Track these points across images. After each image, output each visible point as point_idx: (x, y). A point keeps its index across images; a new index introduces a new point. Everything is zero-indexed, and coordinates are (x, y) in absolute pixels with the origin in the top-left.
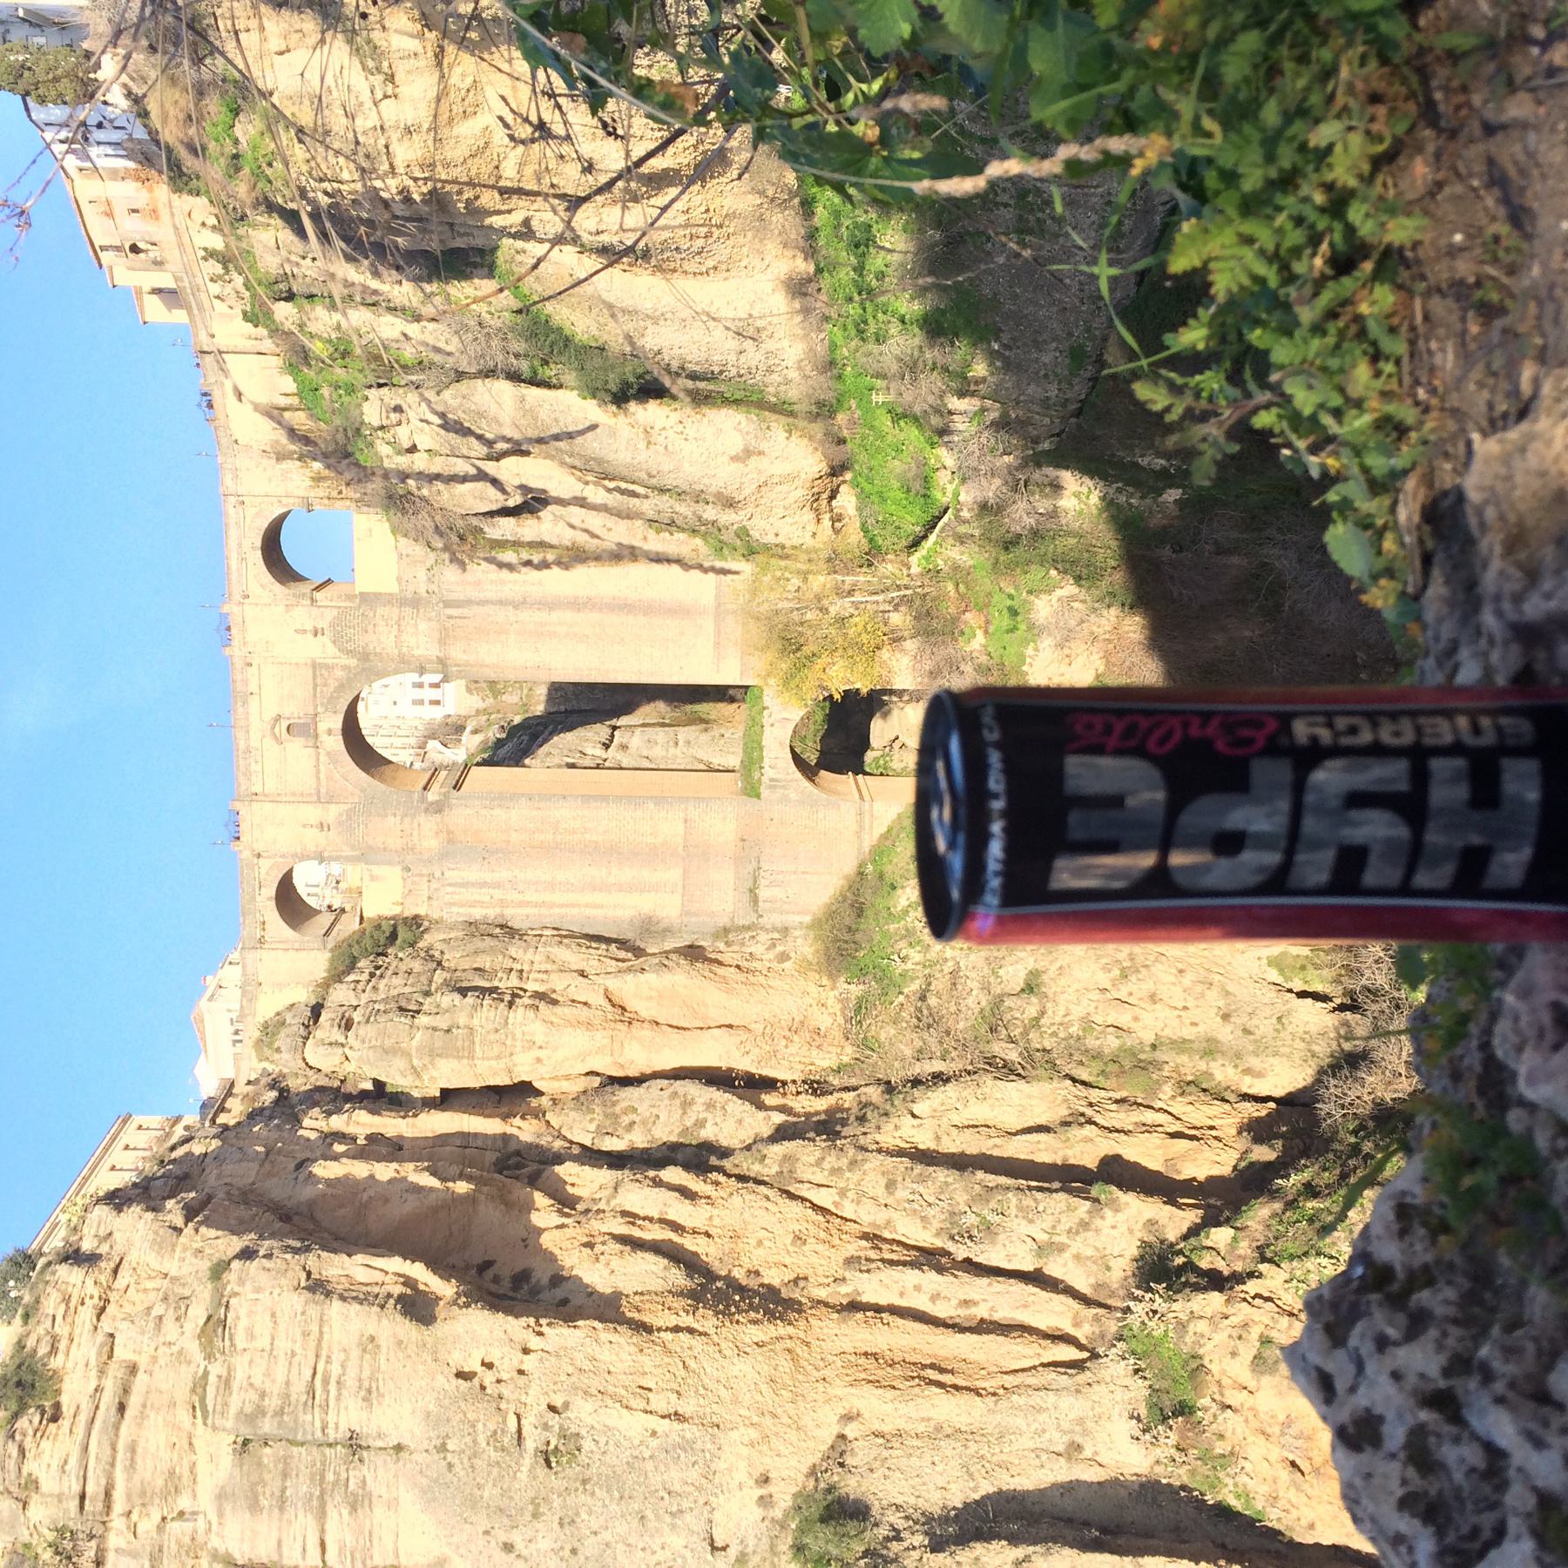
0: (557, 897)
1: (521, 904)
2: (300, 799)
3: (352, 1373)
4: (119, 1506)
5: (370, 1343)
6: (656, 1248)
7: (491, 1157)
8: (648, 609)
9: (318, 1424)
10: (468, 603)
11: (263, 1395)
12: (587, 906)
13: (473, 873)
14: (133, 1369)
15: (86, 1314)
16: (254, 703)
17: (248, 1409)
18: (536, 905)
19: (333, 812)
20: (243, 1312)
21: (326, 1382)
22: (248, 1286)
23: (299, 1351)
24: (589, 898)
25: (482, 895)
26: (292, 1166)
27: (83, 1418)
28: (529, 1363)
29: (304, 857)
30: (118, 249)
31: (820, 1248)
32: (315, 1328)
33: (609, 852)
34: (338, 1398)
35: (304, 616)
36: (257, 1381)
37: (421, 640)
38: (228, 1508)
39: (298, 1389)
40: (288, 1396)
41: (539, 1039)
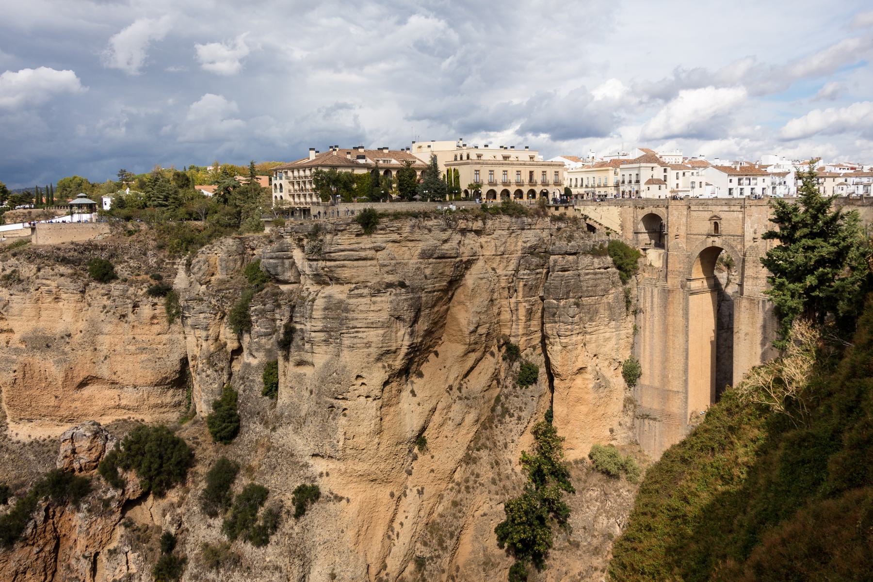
0: (647, 333)
1: (645, 318)
3: (358, 341)
5: (368, 345)
9: (343, 331)
11: (353, 311)
12: (644, 346)
13: (656, 300)
14: (372, 259)
17: (349, 307)
20: (383, 299)
21: (357, 332)
22: (393, 297)
24: (647, 347)
25: (648, 305)
26: (494, 266)
27: (355, 246)
28: (362, 399)
31: (431, 478)
32: (374, 326)
36: (360, 308)
38: (326, 300)
40: (353, 320)
41: (555, 348)
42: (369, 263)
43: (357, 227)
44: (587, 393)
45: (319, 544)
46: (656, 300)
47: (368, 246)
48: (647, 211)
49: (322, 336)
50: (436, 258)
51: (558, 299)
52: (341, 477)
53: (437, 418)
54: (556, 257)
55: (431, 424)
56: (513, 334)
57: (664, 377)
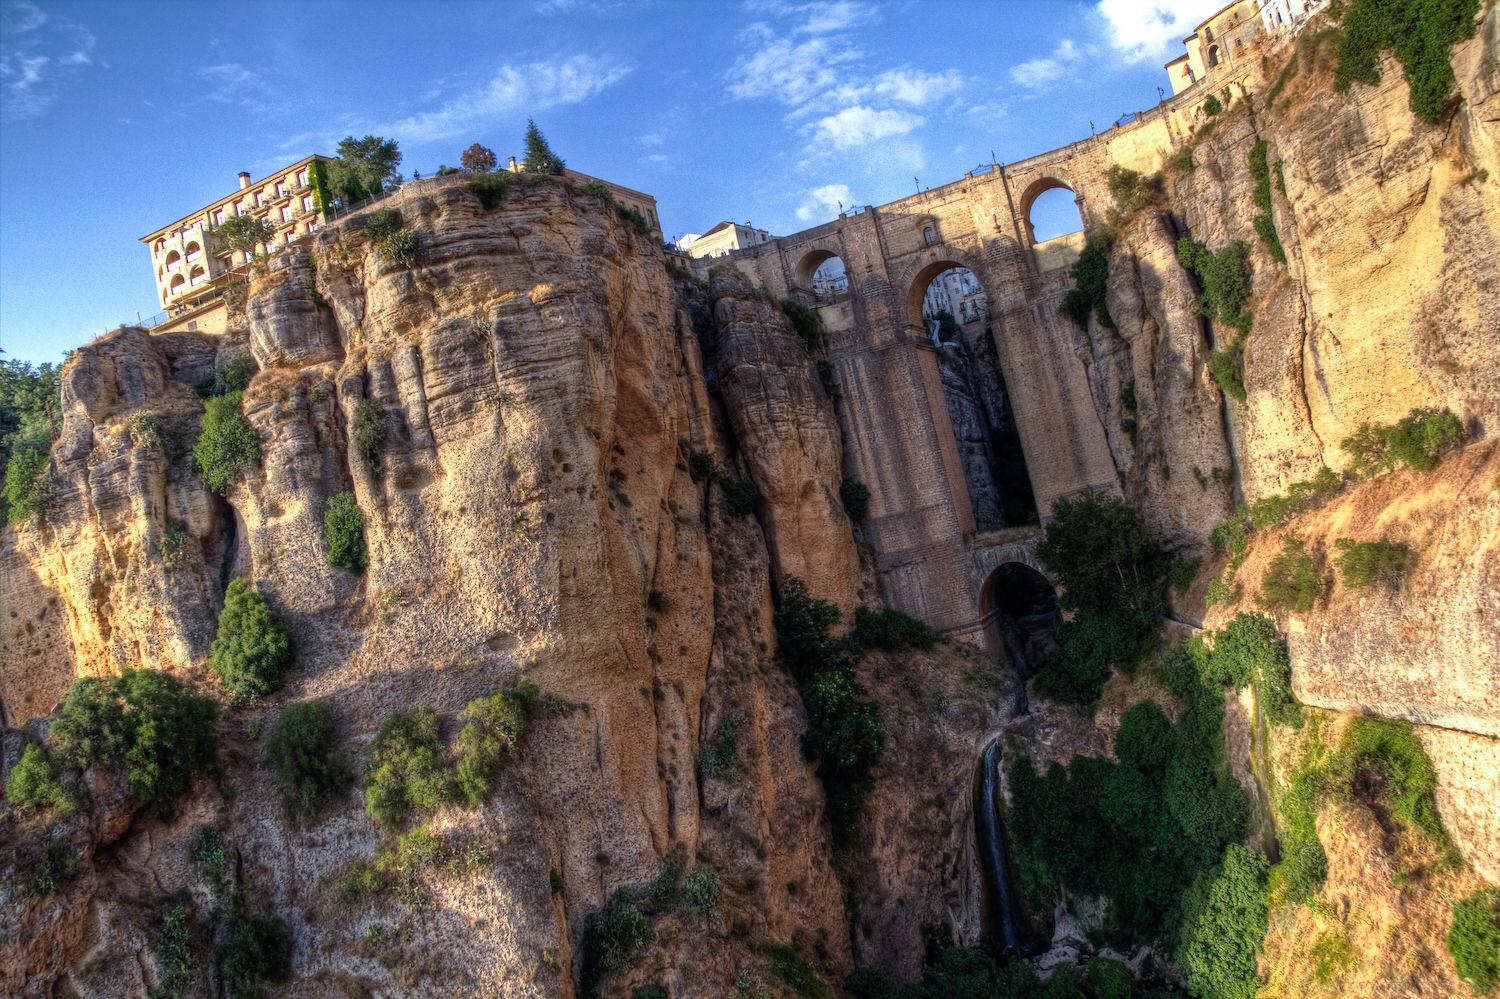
0: (863, 432)
2: (883, 248)
3: (543, 384)
4: (433, 268)
6: (658, 559)
7: (686, 435)
8: (1075, 442)
10: (1044, 321)
13: (863, 374)
14: (513, 251)
15: (540, 212)
16: (937, 202)
17: (507, 328)
18: (854, 420)
19: (882, 272)
22: (578, 305)
23: (549, 346)
24: (868, 454)
25: (852, 386)
27: (480, 231)
28: (574, 496)
29: (846, 261)
30: (1210, 38)
31: (685, 665)
32: (563, 353)
33: (902, 463)
34: (525, 380)
35: (1005, 215)
37: (1009, 296)
39: (527, 354)
41: (770, 446)
42: (511, 258)
43: (472, 201)
44: (823, 527)
45: (564, 800)
46: (863, 374)
47: (502, 230)
48: (803, 251)
49: (455, 400)
50: (606, 256)
51: (756, 361)
52: (561, 666)
53: (669, 555)
54: (730, 299)
55: (662, 564)
56: (696, 438)
57: (908, 491)
